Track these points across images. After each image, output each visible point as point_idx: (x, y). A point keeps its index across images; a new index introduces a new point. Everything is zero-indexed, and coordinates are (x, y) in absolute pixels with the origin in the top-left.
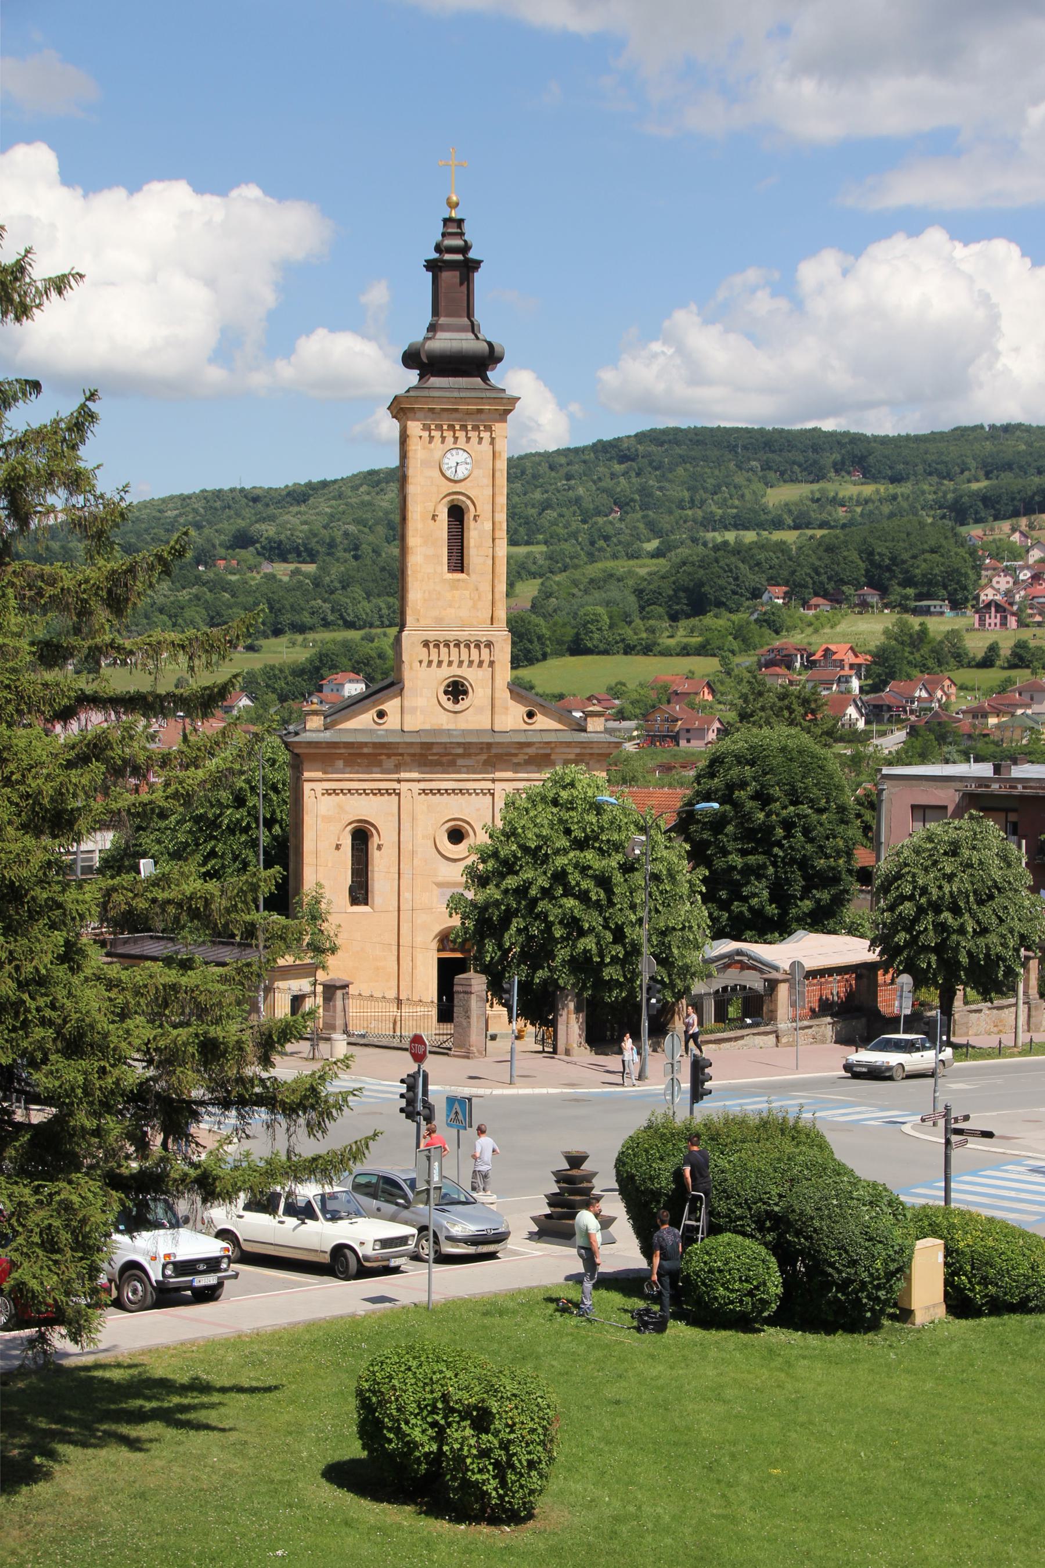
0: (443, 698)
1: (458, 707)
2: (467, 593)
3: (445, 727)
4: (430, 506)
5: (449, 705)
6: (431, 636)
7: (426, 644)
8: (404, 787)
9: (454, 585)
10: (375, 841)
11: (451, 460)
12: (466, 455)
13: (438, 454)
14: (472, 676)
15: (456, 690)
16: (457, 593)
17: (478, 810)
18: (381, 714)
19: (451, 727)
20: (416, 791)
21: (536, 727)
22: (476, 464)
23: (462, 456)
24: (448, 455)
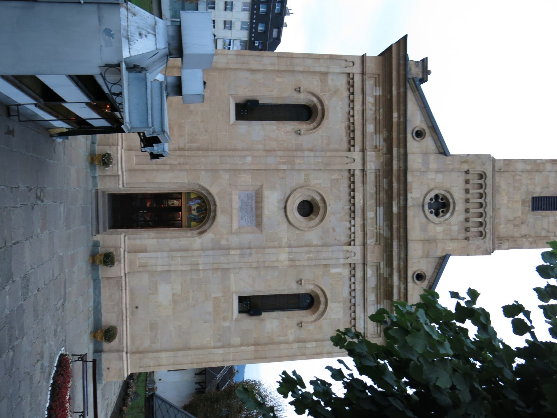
0: (432, 195)
2: (519, 214)
3: (409, 196)
5: (427, 200)
6: (489, 181)
7: (482, 176)
8: (357, 154)
9: (524, 202)
10: (303, 126)
14: (455, 219)
15: (440, 205)
16: (519, 206)
17: (334, 230)
18: (419, 134)
20: (352, 167)
21: (410, 284)
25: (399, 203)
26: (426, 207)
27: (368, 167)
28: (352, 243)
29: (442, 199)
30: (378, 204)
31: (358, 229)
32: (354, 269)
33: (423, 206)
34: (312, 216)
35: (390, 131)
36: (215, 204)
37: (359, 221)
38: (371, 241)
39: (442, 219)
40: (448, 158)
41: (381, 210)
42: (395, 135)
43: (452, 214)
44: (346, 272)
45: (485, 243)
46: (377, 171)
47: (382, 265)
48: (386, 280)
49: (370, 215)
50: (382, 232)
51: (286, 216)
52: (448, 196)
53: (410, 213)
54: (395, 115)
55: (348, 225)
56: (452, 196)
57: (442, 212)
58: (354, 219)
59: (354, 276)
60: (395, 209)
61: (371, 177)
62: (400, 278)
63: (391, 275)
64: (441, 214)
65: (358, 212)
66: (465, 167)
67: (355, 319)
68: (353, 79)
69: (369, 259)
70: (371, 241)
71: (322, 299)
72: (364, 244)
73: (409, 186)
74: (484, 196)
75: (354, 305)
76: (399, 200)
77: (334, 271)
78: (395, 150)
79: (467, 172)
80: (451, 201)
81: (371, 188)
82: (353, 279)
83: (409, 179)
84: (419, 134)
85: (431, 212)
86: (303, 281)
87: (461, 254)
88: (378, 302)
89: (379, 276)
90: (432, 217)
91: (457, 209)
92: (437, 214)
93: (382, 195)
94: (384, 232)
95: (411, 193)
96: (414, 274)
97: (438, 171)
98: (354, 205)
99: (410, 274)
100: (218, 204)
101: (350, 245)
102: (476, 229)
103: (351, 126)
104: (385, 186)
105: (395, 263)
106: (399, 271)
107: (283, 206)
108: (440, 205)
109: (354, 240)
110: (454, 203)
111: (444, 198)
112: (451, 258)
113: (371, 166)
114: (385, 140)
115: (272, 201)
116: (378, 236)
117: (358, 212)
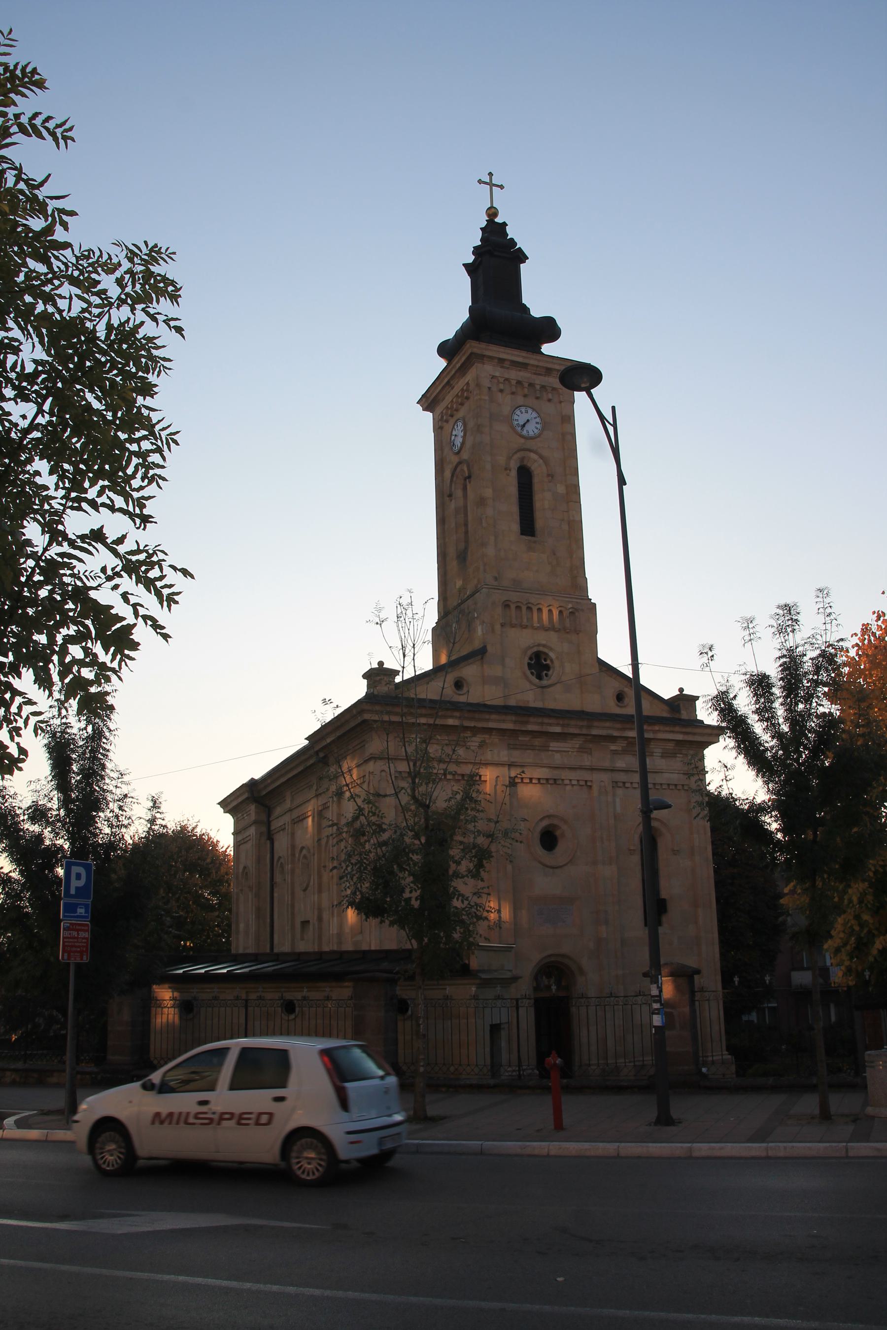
0: (528, 672)
1: (545, 682)
3: (532, 705)
4: (501, 460)
5: (534, 679)
7: (506, 606)
11: (521, 417)
12: (535, 415)
13: (506, 410)
14: (556, 646)
15: (539, 664)
19: (539, 705)
22: (545, 426)
23: (531, 415)
24: (518, 412)
25: (550, 725)
27: (506, 759)
28: (589, 784)
30: (545, 748)
31: (574, 775)
32: (616, 782)
33: (543, 687)
34: (558, 833)
35: (467, 728)
36: (550, 956)
37: (566, 775)
38: (587, 761)
39: (557, 664)
40: (489, 648)
41: (554, 745)
42: (472, 724)
43: (551, 649)
44: (620, 792)
45: (583, 610)
46: (512, 747)
47: (613, 748)
49: (558, 759)
50: (577, 746)
51: (561, 867)
52: (530, 653)
53: (551, 705)
54: (450, 722)
55: (568, 788)
56: (530, 648)
57: (545, 660)
58: (563, 780)
59: (624, 783)
60: (558, 729)
61: (517, 756)
63: (626, 738)
64: (548, 662)
65: (556, 774)
66: (498, 627)
67: (669, 785)
68: (400, 772)
69: (607, 764)
70: (587, 761)
72: (592, 769)
73: (521, 704)
77: (618, 809)
78: (491, 725)
79: (502, 625)
80: (535, 649)
81: (528, 757)
82: (628, 785)
83: (512, 702)
84: (458, 685)
85: (546, 675)
86: (632, 848)
89: (625, 751)
90: (554, 675)
91: (544, 642)
92: (547, 668)
93: (537, 742)
94: (577, 743)
95: (528, 702)
96: (618, 706)
98: (547, 780)
99: (618, 711)
100: (550, 952)
101: (590, 786)
102: (568, 620)
103: (457, 777)
104: (527, 739)
105: (616, 734)
106: (624, 729)
107: (551, 870)
108: (539, 664)
109: (586, 781)
110: (539, 645)
112: (601, 655)
113: (504, 755)
114: (474, 735)
115: (545, 884)
116: (582, 750)
117: (556, 774)
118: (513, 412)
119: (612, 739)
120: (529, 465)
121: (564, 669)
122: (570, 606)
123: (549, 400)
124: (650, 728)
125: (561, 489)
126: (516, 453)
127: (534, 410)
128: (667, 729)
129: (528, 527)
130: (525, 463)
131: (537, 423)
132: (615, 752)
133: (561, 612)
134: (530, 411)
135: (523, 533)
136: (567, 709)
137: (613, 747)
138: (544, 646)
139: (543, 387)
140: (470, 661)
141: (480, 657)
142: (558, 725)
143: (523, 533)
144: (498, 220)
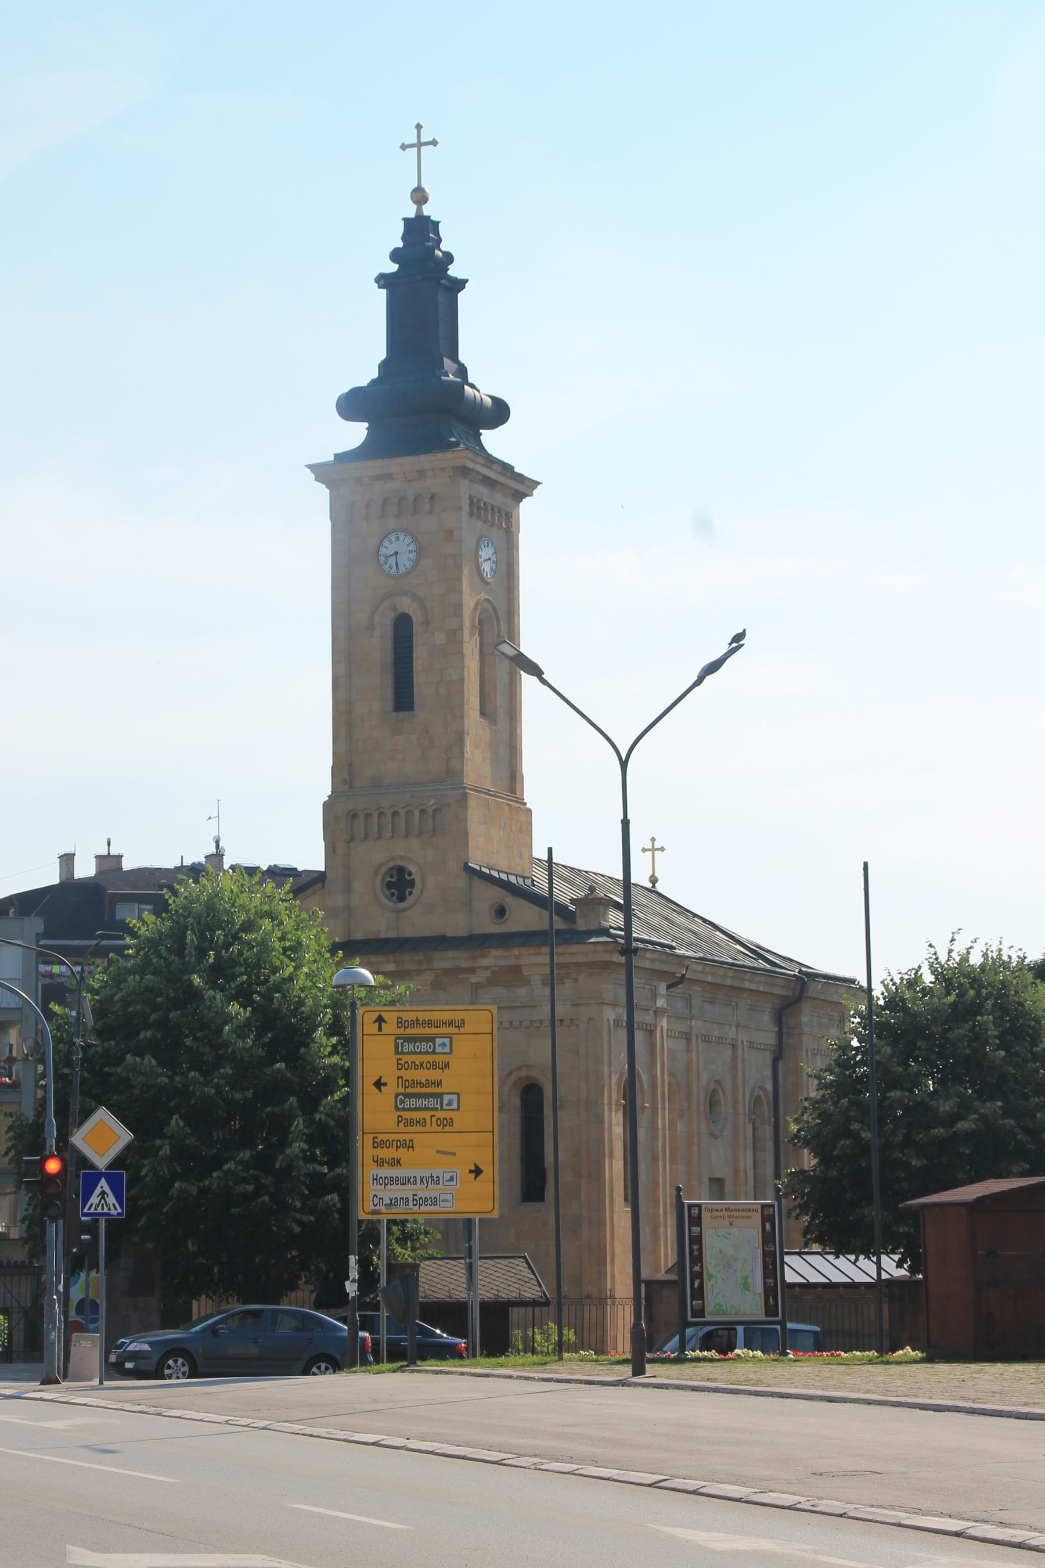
3: (382, 936)
12: (408, 540)
15: (399, 883)
19: (392, 934)
22: (421, 552)
24: (386, 543)
25: (381, 963)
26: (402, 905)
29: (392, 876)
33: (398, 912)
40: (329, 876)
45: (448, 805)
47: (474, 979)
48: (493, 972)
52: (384, 870)
53: (408, 932)
56: (382, 865)
62: (484, 956)
63: (486, 968)
71: (524, 1073)
73: (371, 937)
74: (382, 810)
75: (532, 1021)
76: (377, 963)
80: (391, 864)
83: (359, 936)
87: (466, 845)
88: (527, 982)
91: (402, 854)
97: (348, 889)
99: (494, 929)
105: (465, 964)
110: (393, 859)
111: (390, 873)
118: (380, 544)
119: (472, 970)
120: (406, 611)
121: (430, 885)
122: (432, 802)
123: (430, 513)
124: (506, 954)
125: (440, 638)
126: (382, 600)
127: (407, 532)
128: (532, 951)
129: (403, 697)
130: (400, 610)
131: (410, 552)
132: (477, 986)
133: (423, 812)
134: (402, 537)
135: (397, 708)
136: (428, 935)
137: (474, 979)
138: (401, 858)
139: (418, 499)
140: (309, 891)
141: (319, 885)
142: (389, 962)
143: (397, 708)
144: (427, 210)
